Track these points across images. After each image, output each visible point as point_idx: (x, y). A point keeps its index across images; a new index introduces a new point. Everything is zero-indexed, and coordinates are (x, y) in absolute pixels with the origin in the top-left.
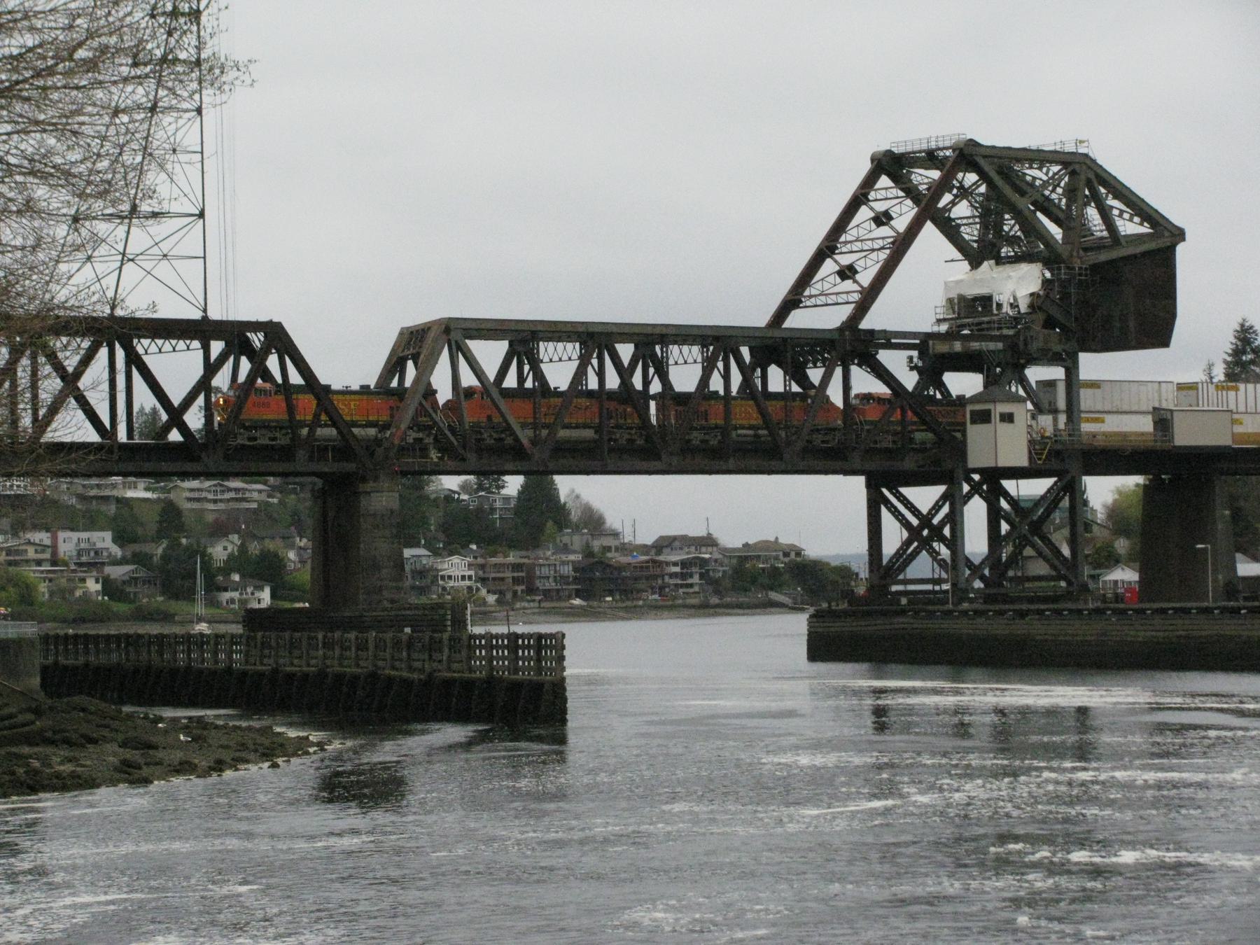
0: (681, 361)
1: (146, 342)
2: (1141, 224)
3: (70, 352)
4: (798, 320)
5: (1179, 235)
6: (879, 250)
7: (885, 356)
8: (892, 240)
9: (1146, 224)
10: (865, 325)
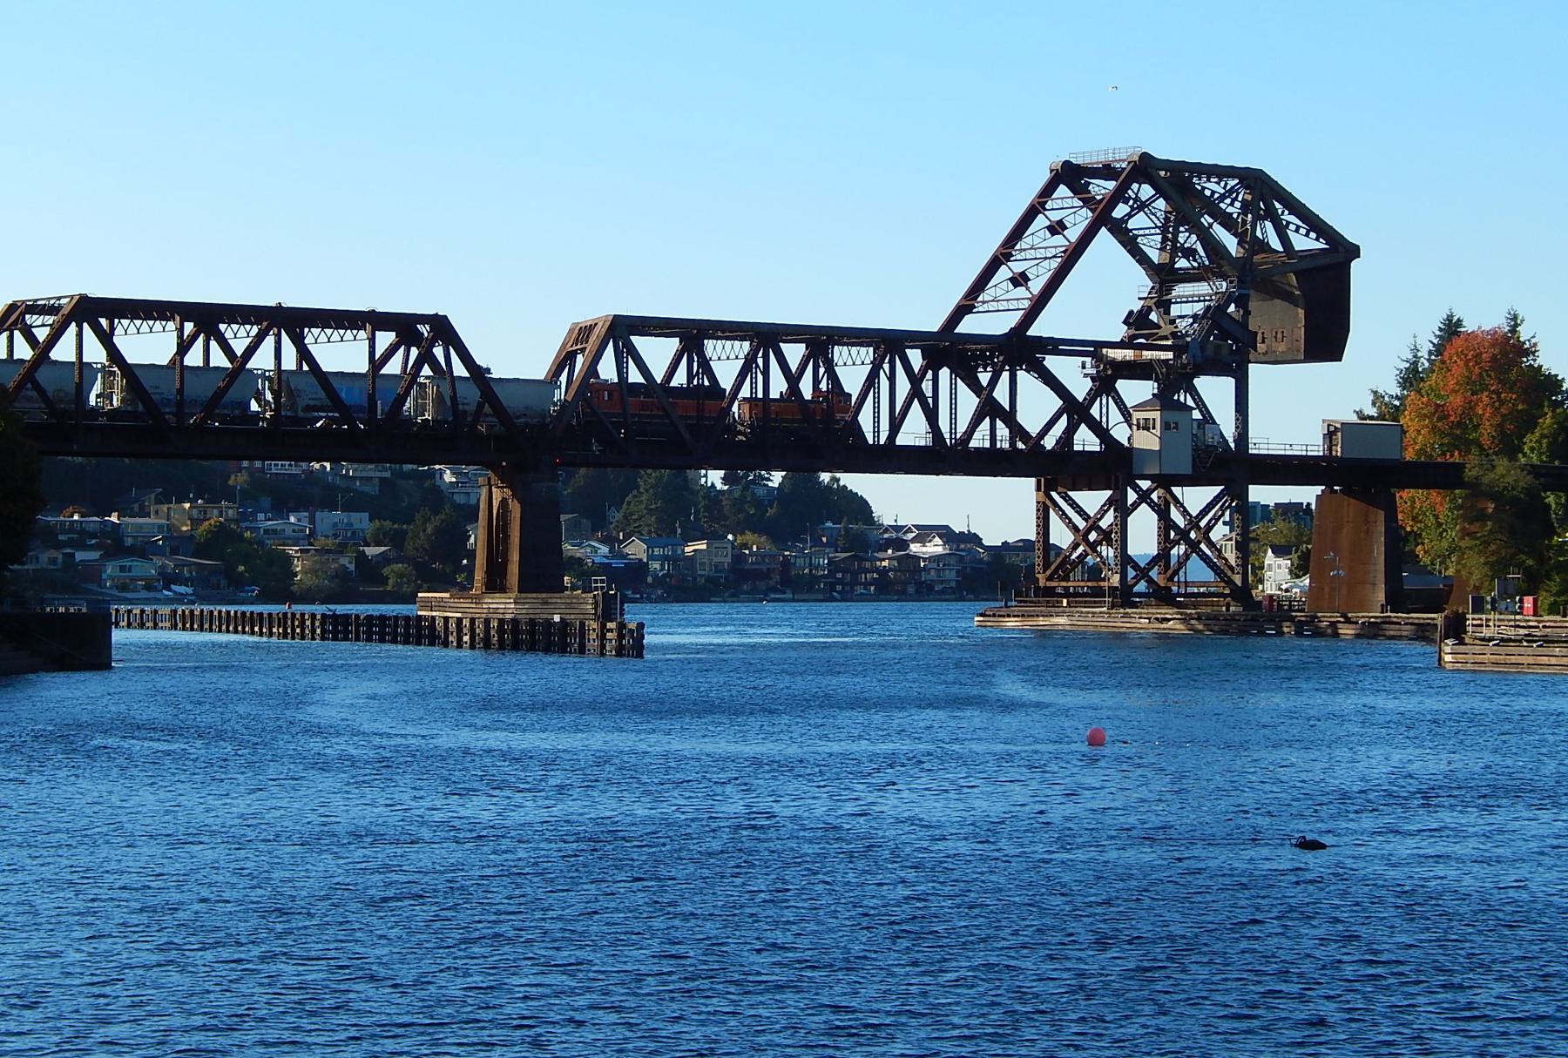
0: (850, 362)
1: (316, 331)
2: (1317, 239)
3: (240, 335)
4: (969, 325)
5: (1354, 251)
6: (1050, 258)
7: (1052, 362)
8: (1064, 249)
9: (1321, 240)
10: (1033, 331)
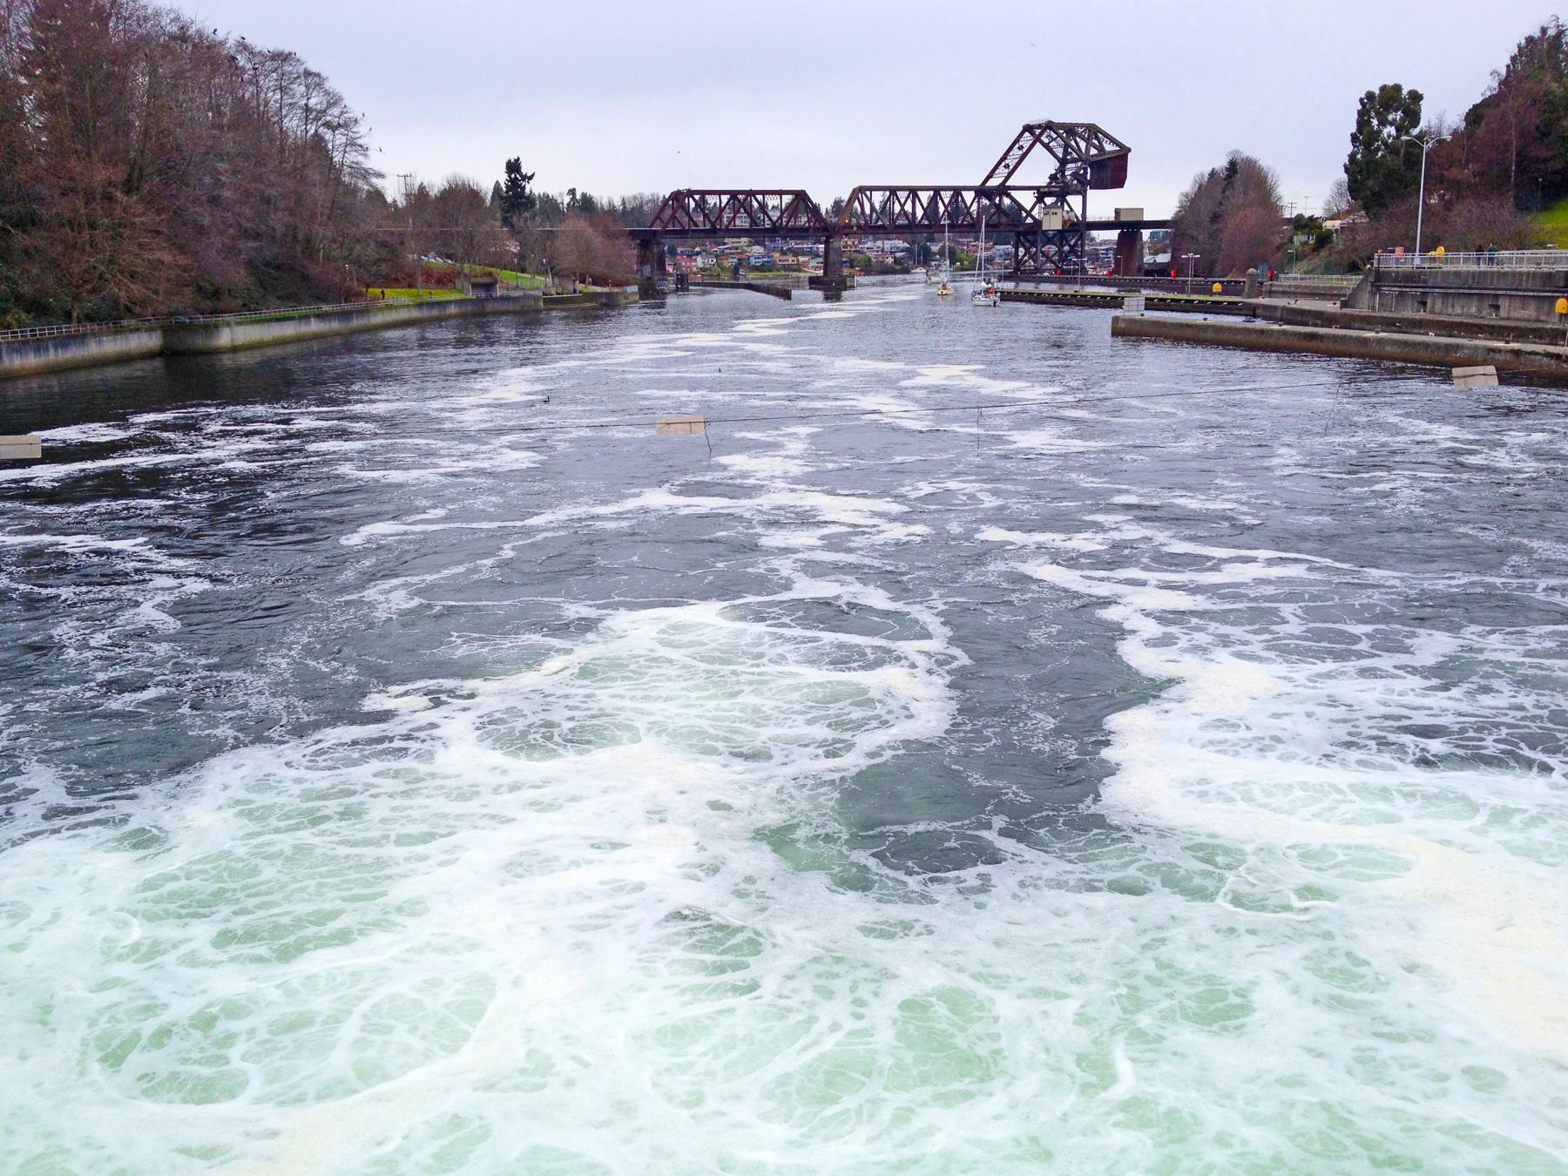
5: (1129, 150)
